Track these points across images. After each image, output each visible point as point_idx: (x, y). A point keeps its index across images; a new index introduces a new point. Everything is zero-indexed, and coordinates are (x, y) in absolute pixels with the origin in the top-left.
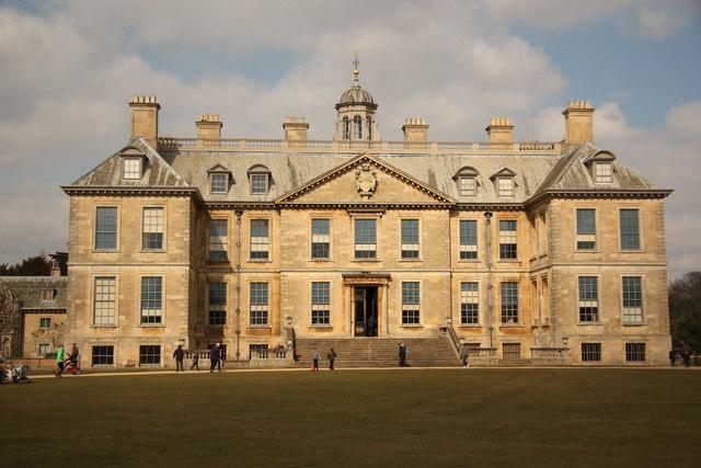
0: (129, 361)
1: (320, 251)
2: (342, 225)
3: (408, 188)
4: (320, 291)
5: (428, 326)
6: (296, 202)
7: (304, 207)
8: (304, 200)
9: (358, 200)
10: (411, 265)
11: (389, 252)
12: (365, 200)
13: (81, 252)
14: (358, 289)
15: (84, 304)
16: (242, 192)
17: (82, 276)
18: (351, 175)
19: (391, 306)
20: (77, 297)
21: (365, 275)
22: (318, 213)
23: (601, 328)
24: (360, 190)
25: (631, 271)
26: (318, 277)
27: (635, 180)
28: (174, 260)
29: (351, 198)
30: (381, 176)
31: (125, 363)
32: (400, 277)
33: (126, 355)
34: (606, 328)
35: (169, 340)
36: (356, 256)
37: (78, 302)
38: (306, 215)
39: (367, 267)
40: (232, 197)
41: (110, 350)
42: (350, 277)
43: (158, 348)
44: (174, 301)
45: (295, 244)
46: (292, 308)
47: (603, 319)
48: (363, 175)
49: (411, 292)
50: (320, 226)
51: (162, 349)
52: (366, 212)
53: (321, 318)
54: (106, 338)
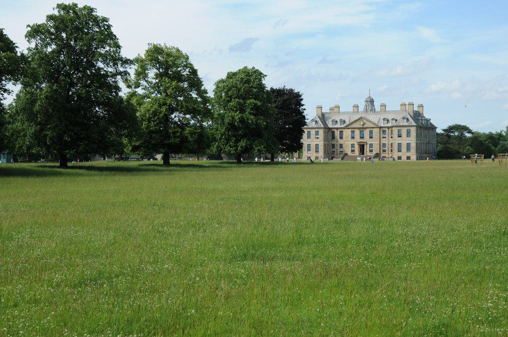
1: (353, 138)
2: (357, 132)
4: (353, 146)
7: (349, 128)
14: (360, 145)
16: (338, 126)
19: (367, 148)
22: (352, 130)
25: (409, 142)
26: (352, 143)
30: (365, 121)
32: (369, 143)
38: (350, 130)
39: (362, 141)
40: (336, 126)
49: (371, 145)
50: (353, 132)
52: (362, 129)
53: (353, 151)
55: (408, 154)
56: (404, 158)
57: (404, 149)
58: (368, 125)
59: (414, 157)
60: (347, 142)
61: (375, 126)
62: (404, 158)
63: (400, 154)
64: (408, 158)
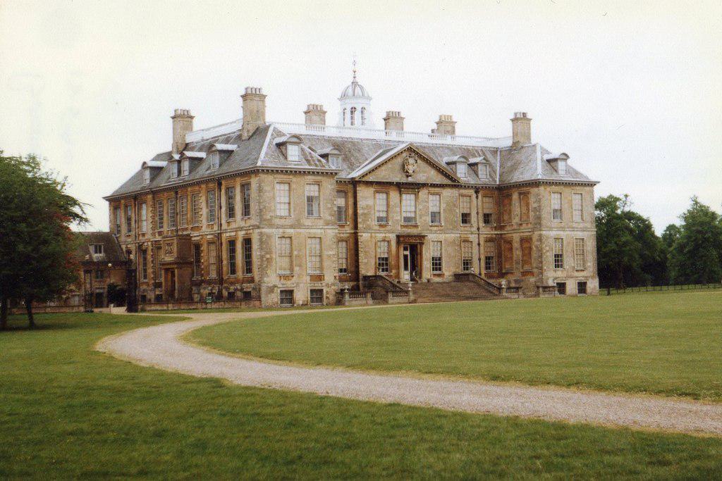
0: (304, 301)
3: (433, 172)
5: (448, 271)
6: (366, 179)
8: (371, 178)
9: (404, 180)
10: (435, 228)
11: (424, 218)
12: (410, 180)
13: (268, 217)
15: (271, 258)
17: (269, 236)
18: (399, 160)
20: (267, 253)
21: (409, 236)
23: (565, 272)
24: (407, 172)
25: (580, 234)
27: (577, 173)
28: (328, 224)
29: (398, 178)
30: (419, 161)
31: (301, 303)
33: (301, 296)
34: (568, 272)
35: (327, 285)
36: (405, 221)
37: (268, 256)
41: (291, 292)
42: (403, 236)
43: (321, 291)
44: (329, 256)
45: (366, 211)
46: (366, 261)
47: (566, 266)
48: (411, 161)
51: (325, 292)
54: (289, 285)
55: (581, 276)
56: (571, 287)
57: (569, 262)
58: (424, 174)
59: (593, 284)
60: (364, 235)
61: (439, 179)
62: (571, 287)
63: (560, 274)
64: (582, 287)
